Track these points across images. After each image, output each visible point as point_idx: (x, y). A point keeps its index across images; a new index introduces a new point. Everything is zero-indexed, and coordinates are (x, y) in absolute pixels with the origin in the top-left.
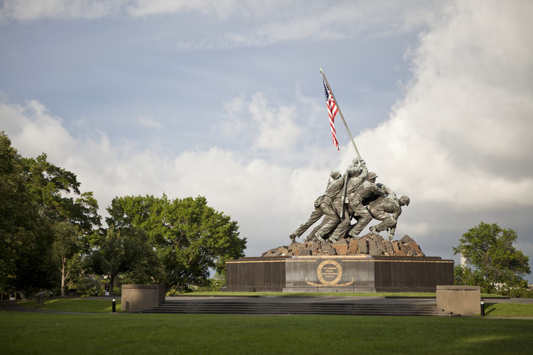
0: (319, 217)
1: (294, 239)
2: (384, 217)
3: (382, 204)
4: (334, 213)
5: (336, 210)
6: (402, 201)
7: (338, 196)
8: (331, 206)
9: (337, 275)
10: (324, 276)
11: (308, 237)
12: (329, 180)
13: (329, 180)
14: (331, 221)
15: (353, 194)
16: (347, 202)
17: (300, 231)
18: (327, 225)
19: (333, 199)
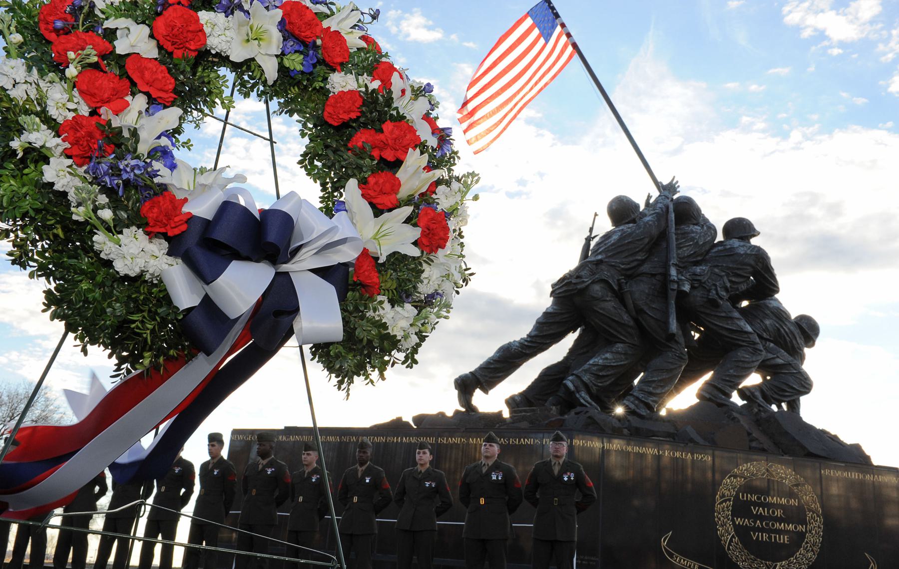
0: (557, 337)
1: (471, 394)
2: (780, 361)
3: (767, 322)
4: (632, 323)
5: (640, 311)
6: (804, 326)
7: (646, 268)
8: (620, 296)
9: (802, 535)
10: (742, 532)
11: (525, 395)
12: (591, 230)
13: (591, 230)
14: (620, 347)
15: (698, 269)
16: (687, 288)
17: (496, 370)
18: (608, 355)
19: (631, 275)
